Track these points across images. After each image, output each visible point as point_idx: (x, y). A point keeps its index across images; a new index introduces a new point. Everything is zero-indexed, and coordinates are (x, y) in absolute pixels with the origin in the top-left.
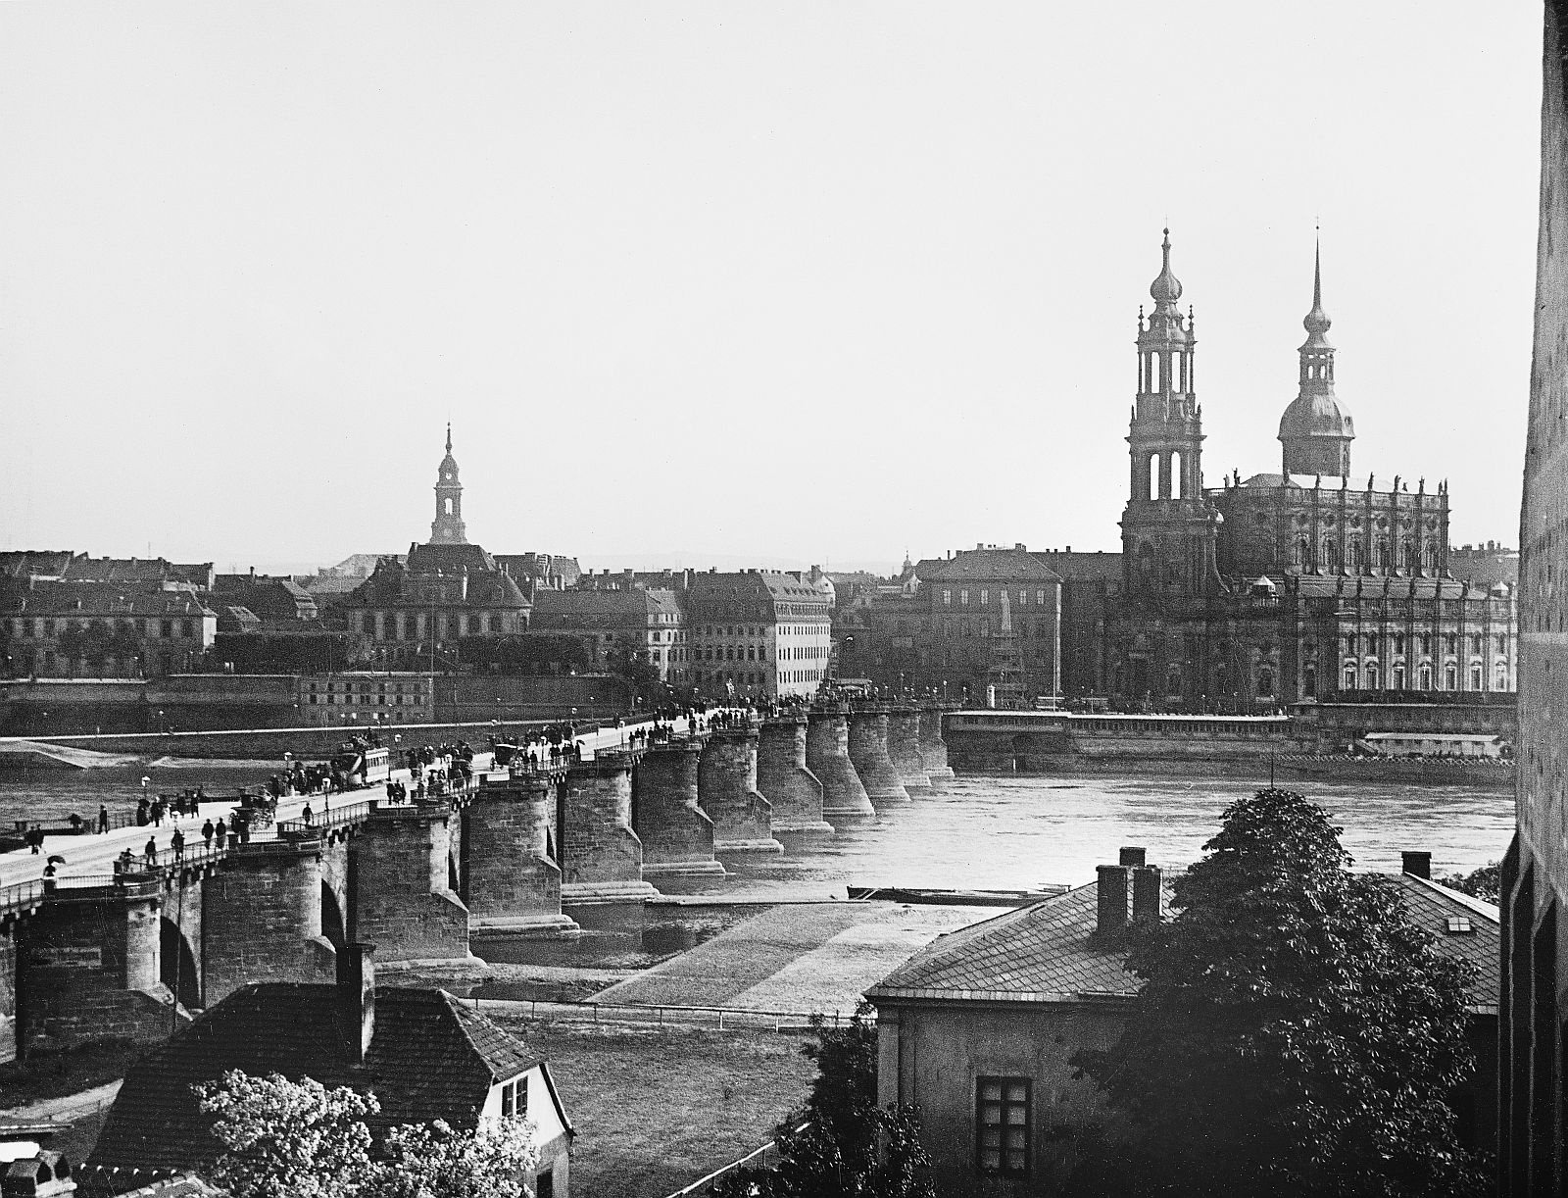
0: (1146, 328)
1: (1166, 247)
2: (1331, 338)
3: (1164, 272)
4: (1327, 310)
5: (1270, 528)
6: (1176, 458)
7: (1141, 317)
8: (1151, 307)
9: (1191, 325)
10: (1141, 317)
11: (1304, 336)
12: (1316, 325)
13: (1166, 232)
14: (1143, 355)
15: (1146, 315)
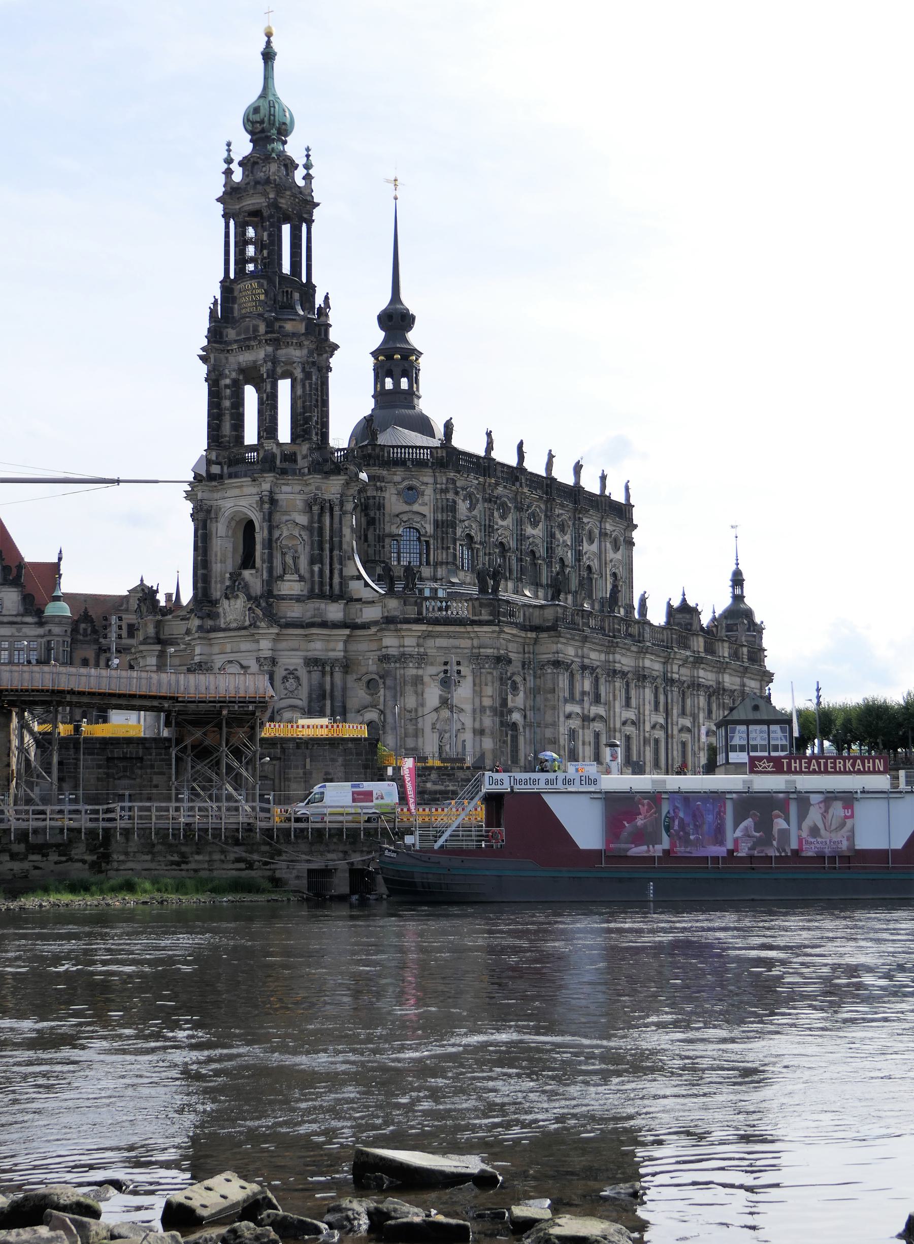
0: (238, 176)
1: (268, 56)
2: (414, 337)
3: (264, 95)
4: (409, 301)
5: (425, 510)
6: (284, 387)
7: (229, 161)
8: (244, 146)
9: (308, 178)
10: (229, 161)
11: (378, 336)
12: (396, 320)
13: (269, 35)
14: (232, 223)
15: (237, 157)
